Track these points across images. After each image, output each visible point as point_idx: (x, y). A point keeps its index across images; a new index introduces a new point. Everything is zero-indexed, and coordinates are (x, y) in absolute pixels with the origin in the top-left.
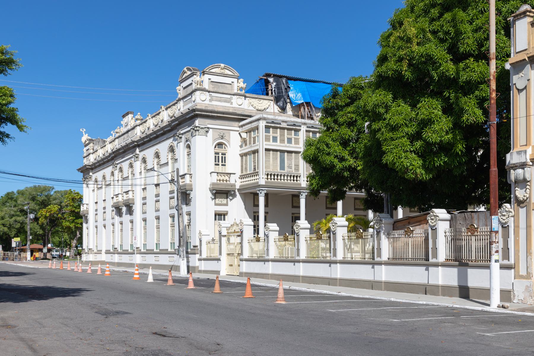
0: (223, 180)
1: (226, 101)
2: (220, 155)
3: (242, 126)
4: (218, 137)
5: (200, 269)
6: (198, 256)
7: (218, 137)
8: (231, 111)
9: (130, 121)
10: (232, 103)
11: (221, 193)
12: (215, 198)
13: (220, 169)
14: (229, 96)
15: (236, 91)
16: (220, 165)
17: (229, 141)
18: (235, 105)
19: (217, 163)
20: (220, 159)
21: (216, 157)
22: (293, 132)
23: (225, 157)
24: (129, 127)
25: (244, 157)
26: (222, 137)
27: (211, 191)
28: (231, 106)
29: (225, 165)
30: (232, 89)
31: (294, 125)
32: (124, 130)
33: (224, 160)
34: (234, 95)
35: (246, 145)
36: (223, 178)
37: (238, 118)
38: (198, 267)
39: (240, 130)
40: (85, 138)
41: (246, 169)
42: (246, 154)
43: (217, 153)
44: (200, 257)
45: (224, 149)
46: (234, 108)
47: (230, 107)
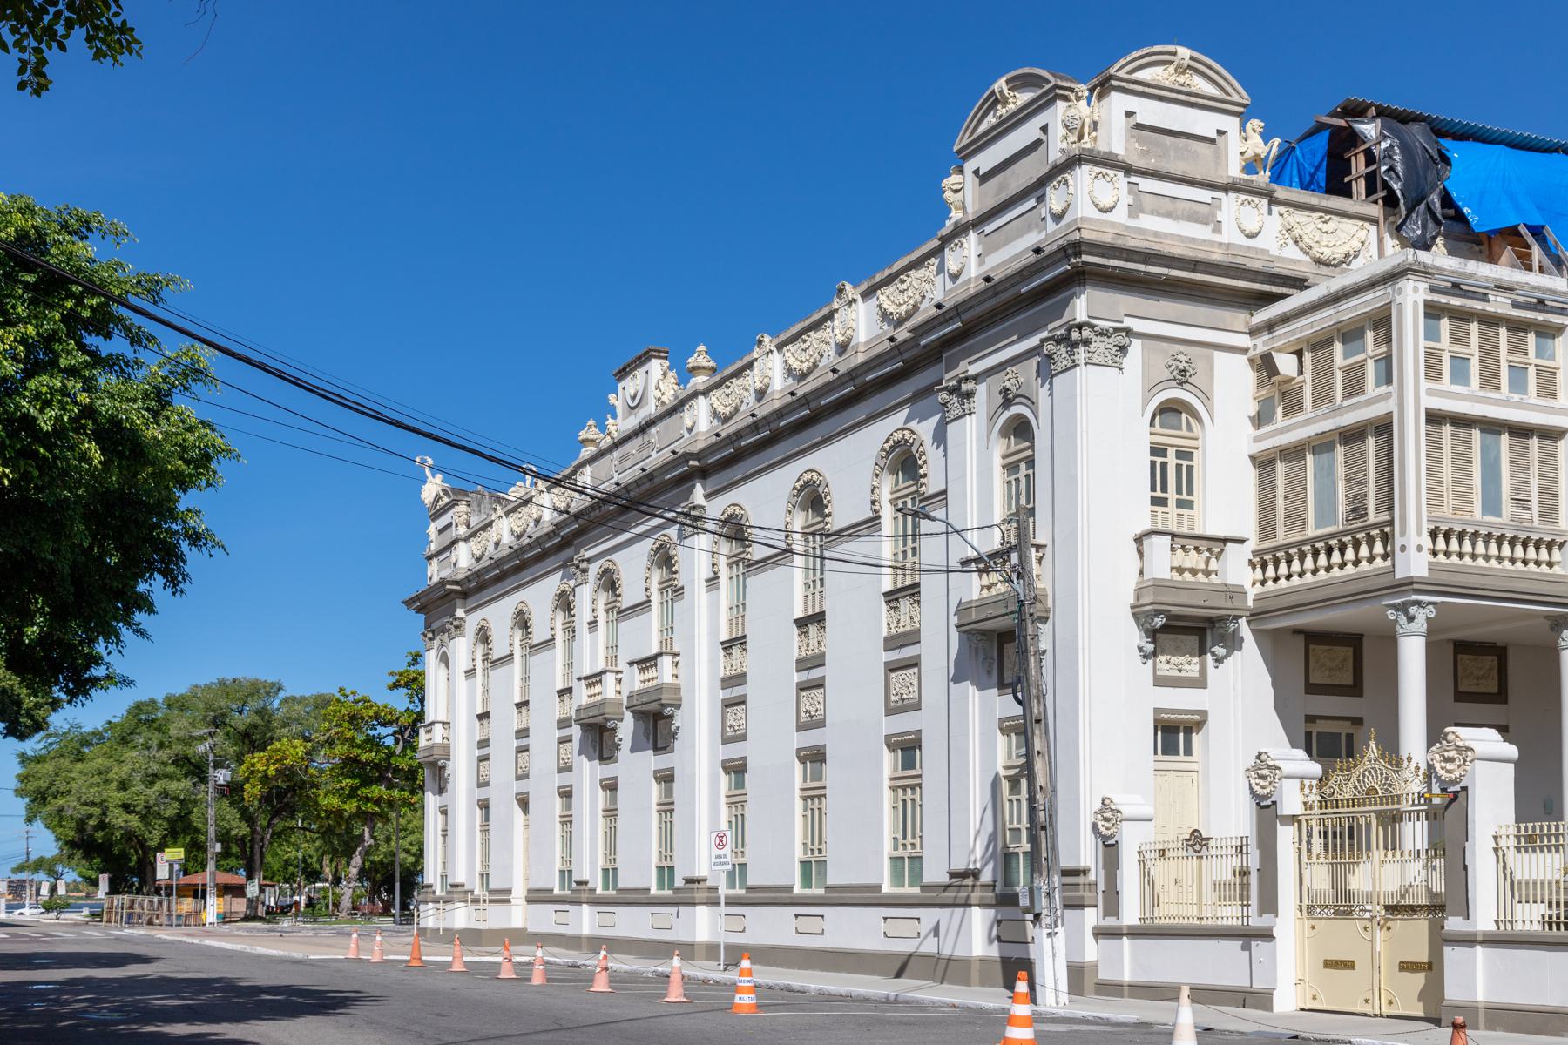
0: (1194, 572)
1: (1194, 218)
2: (1172, 460)
3: (1270, 326)
4: (1166, 374)
5: (1105, 975)
6: (1091, 917)
7: (1166, 374)
8: (1217, 256)
9: (655, 382)
10: (1218, 227)
11: (1183, 629)
12: (1155, 654)
13: (1172, 518)
14: (1205, 195)
15: (1234, 170)
16: (1172, 503)
17: (1207, 397)
18: (1230, 235)
19: (1159, 493)
20: (1171, 475)
21: (1153, 464)
22: (1531, 337)
23: (1190, 468)
24: (651, 409)
25: (1280, 467)
26: (1182, 377)
27: (1139, 615)
28: (1216, 238)
29: (1187, 505)
30: (1220, 158)
31: (1541, 305)
32: (622, 424)
33: (1187, 480)
34: (1226, 188)
35: (1293, 407)
36: (1193, 560)
37: (1253, 290)
38: (1095, 966)
39: (1261, 344)
40: (432, 488)
41: (1296, 518)
42: (1293, 453)
43: (1158, 451)
44: (1111, 922)
45: (1184, 432)
46: (1229, 245)
47: (1212, 243)
